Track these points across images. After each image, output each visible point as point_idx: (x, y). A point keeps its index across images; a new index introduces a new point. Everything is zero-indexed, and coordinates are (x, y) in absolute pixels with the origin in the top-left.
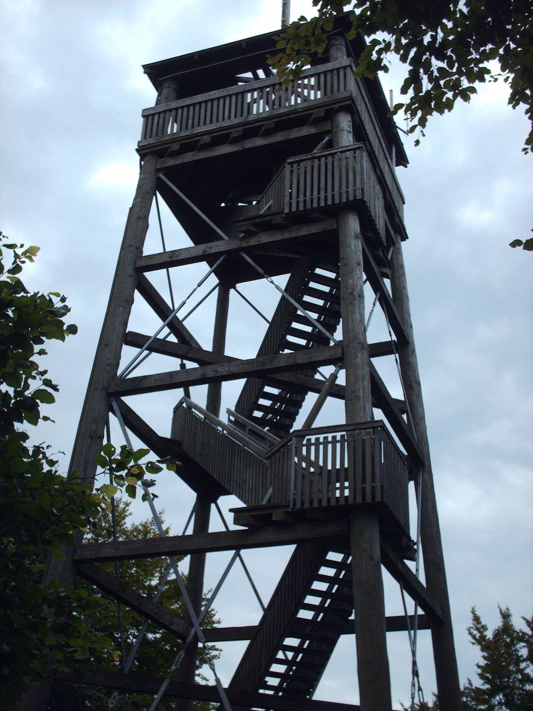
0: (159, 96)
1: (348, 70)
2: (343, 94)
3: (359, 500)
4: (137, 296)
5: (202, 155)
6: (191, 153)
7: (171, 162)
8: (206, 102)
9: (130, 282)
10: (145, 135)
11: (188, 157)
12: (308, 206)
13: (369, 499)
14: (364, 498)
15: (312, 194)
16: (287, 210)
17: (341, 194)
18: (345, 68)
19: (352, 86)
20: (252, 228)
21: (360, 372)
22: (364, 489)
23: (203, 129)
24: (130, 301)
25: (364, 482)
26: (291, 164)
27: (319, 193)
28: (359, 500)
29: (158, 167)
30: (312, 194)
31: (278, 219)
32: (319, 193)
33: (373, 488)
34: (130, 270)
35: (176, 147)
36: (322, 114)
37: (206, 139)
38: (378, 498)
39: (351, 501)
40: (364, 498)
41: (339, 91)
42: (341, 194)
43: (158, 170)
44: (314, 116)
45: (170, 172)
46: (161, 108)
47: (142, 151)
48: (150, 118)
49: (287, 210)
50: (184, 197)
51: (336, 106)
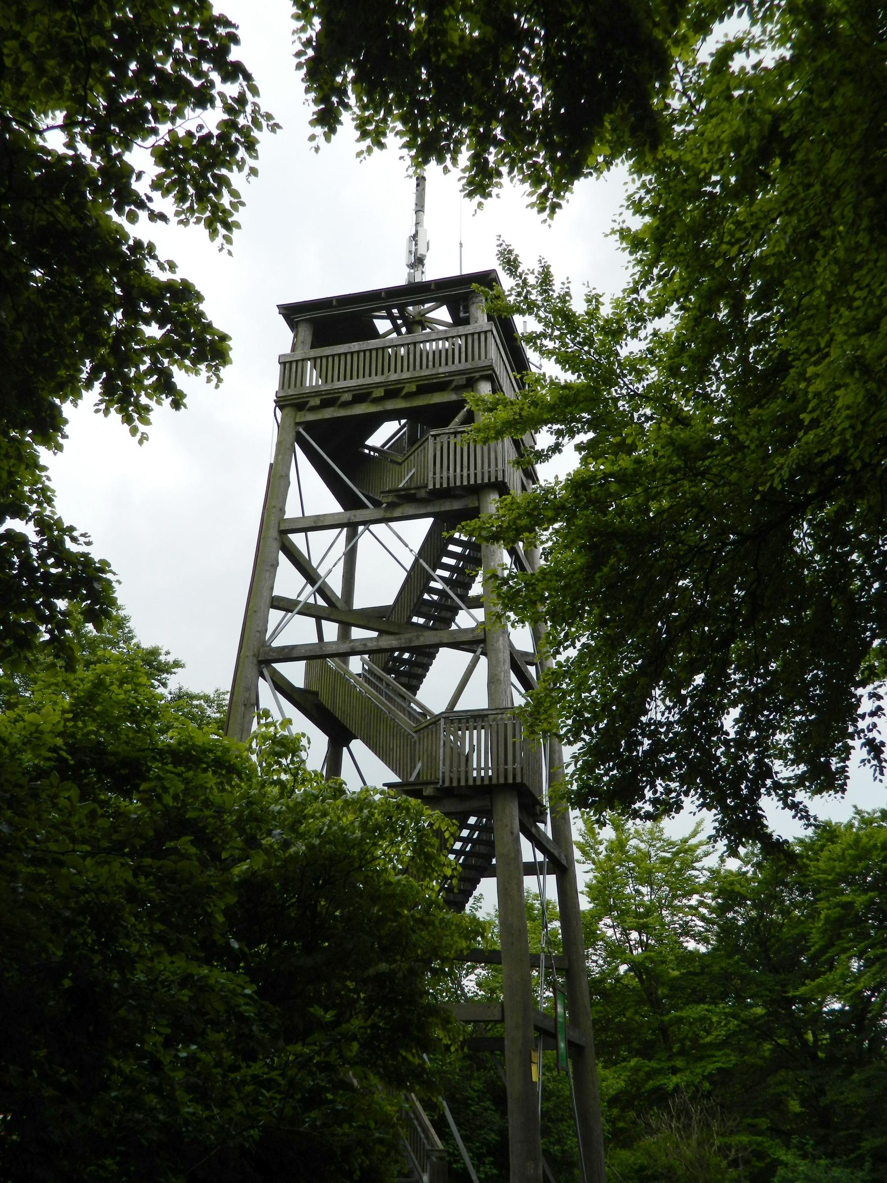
0: (295, 336)
1: (489, 335)
2: (483, 363)
3: (502, 781)
4: (282, 557)
5: (342, 413)
6: (331, 409)
7: (311, 417)
8: (346, 354)
9: (276, 545)
10: (282, 385)
11: (328, 413)
12: (452, 485)
13: (510, 781)
14: (506, 778)
15: (455, 471)
16: (431, 487)
17: (483, 473)
18: (486, 332)
19: (493, 353)
20: (396, 500)
21: (501, 655)
22: (506, 770)
23: (342, 384)
24: (275, 565)
25: (506, 763)
26: (435, 436)
27: (462, 470)
28: (502, 781)
29: (298, 420)
30: (455, 471)
31: (422, 494)
32: (462, 470)
33: (514, 769)
34: (273, 533)
35: (316, 401)
36: (463, 382)
37: (347, 397)
38: (519, 780)
39: (494, 781)
40: (506, 778)
41: (480, 358)
42: (483, 473)
43: (298, 424)
44: (454, 384)
45: (309, 427)
46: (299, 355)
47: (281, 403)
48: (287, 365)
49: (431, 487)
50: (325, 456)
51: (477, 375)
